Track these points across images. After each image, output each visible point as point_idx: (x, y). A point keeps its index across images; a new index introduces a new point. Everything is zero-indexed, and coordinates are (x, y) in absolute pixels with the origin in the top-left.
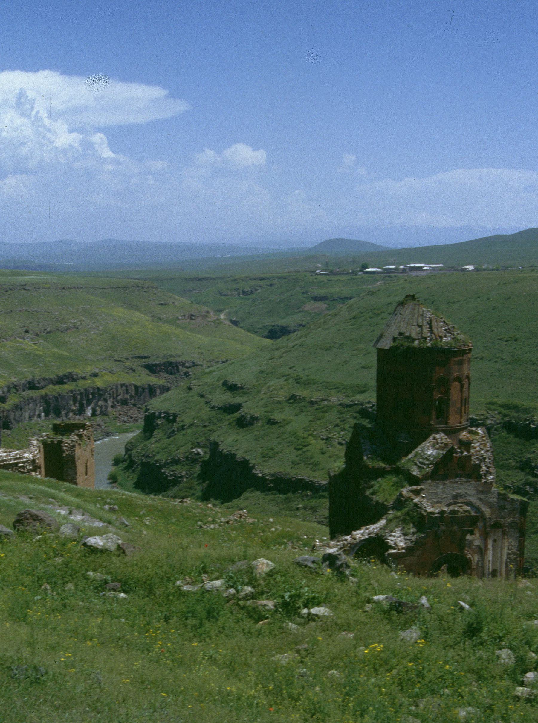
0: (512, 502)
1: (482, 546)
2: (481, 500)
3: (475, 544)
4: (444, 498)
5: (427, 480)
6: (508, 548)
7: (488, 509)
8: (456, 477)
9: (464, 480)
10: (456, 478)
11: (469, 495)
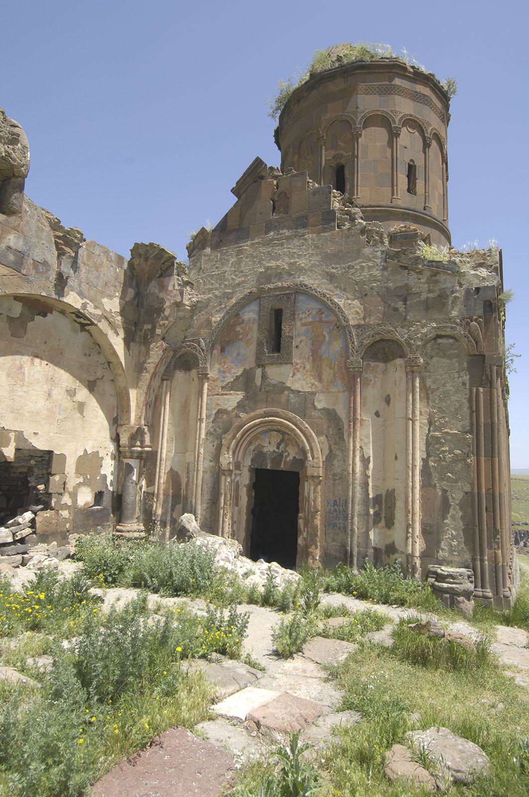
0: (435, 274)
1: (342, 413)
2: (332, 278)
3: (319, 406)
4: (238, 285)
5: (204, 248)
6: (430, 423)
7: (356, 302)
8: (268, 229)
9: (286, 232)
10: (266, 233)
11: (301, 270)
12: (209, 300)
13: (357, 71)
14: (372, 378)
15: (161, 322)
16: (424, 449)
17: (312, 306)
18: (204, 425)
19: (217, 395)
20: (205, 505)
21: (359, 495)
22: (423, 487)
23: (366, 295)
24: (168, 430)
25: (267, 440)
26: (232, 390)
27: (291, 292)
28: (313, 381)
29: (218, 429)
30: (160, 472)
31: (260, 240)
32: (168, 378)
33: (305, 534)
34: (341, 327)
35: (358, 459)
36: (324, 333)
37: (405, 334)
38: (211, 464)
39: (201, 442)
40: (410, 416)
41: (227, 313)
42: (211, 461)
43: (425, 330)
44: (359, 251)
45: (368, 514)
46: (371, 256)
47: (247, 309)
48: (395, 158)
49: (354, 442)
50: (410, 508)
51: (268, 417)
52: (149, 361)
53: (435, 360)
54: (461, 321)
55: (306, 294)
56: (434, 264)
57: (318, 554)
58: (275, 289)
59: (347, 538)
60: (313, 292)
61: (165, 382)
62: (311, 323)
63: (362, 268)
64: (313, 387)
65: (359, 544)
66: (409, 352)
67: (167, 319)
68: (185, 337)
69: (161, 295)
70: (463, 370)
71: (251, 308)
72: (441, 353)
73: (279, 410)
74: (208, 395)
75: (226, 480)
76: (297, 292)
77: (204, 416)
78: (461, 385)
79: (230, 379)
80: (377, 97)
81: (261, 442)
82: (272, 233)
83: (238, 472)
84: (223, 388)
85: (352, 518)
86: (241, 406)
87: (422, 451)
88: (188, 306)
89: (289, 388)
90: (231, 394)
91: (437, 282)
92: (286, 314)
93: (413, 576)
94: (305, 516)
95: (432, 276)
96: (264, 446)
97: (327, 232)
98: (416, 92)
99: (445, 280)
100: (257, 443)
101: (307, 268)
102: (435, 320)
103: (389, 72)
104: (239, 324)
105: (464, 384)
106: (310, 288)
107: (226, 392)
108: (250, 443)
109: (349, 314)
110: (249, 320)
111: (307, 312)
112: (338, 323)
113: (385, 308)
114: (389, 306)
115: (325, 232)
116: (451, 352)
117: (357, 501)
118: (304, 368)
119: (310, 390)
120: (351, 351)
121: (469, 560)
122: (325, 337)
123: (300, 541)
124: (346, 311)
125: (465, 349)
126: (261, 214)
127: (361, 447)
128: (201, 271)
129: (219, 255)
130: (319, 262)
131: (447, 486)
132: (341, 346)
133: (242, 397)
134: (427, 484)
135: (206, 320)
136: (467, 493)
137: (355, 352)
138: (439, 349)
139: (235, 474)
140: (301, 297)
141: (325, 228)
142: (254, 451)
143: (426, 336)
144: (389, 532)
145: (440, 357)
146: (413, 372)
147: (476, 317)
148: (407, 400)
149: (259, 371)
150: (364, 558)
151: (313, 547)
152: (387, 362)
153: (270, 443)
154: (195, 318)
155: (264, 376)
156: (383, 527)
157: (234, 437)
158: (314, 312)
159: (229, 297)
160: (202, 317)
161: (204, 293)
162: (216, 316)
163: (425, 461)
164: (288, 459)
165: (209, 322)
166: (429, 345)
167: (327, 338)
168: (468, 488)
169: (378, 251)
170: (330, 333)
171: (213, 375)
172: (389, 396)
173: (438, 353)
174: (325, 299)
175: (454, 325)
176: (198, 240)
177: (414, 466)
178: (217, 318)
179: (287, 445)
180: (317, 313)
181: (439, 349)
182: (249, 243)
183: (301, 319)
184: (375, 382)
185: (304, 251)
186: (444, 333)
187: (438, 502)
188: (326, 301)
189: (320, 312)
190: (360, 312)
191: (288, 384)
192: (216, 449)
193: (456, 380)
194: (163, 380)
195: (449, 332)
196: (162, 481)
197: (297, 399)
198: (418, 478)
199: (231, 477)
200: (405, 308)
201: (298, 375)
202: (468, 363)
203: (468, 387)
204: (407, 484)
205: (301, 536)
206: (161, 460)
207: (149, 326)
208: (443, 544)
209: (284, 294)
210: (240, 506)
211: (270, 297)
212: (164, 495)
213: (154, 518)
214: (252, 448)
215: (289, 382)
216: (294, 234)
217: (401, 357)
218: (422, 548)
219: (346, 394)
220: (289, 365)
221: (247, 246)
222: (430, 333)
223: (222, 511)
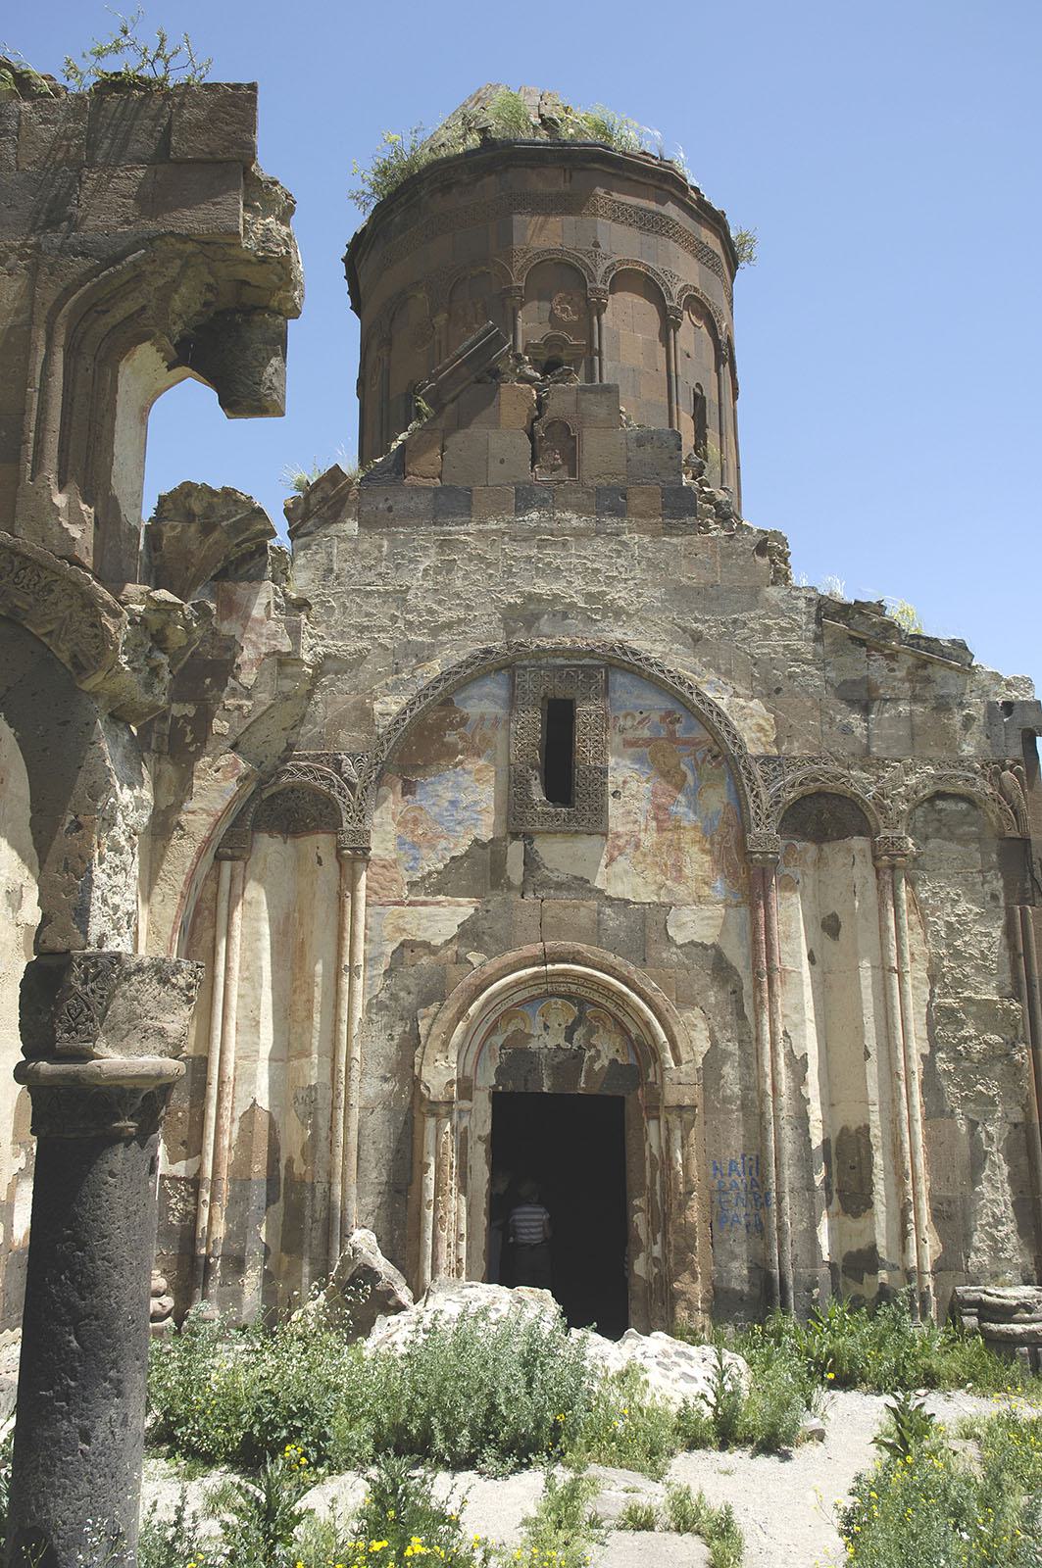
0: (924, 664)
1: (736, 955)
3: (680, 939)
4: (449, 626)
5: (336, 517)
6: (934, 977)
7: (756, 704)
9: (575, 520)
10: (520, 510)
12: (361, 657)
13: (596, 166)
14: (799, 877)
15: (230, 702)
16: (925, 1035)
17: (648, 702)
18: (359, 984)
19: (396, 904)
20: (371, 1201)
21: (789, 1147)
22: (927, 1117)
23: (778, 691)
24: (240, 996)
25: (539, 1019)
26: (439, 892)
27: (596, 662)
28: (660, 878)
29: (402, 994)
30: (219, 1116)
31: (503, 525)
32: (237, 854)
33: (657, 1250)
34: (721, 754)
35: (782, 1062)
36: (683, 767)
37: (870, 783)
38: (387, 1087)
39: (356, 1030)
40: (894, 964)
41: (422, 695)
42: (385, 1079)
43: (912, 780)
44: (755, 591)
45: (810, 1186)
46: (783, 606)
47: (473, 691)
48: (673, 374)
49: (772, 1021)
50: (908, 1165)
51: (554, 962)
52: (190, 805)
53: (933, 843)
54: (983, 767)
55: (633, 672)
56: (922, 642)
57: (698, 1290)
58: (555, 652)
59: (768, 1247)
60: (655, 670)
61: (227, 866)
62: (648, 742)
63: (767, 630)
64: (662, 892)
65: (795, 1260)
66: (882, 824)
67: (249, 697)
68: (290, 747)
69: (226, 628)
70: (991, 868)
71: (486, 690)
72: (944, 830)
73: (582, 947)
74: (367, 905)
75: (438, 1129)
76: (611, 665)
77: (360, 960)
78: (988, 899)
79: (433, 862)
80: (633, 232)
81: (521, 1026)
82: (535, 515)
83: (466, 1104)
84: (412, 885)
85: (780, 1201)
86: (469, 934)
87: (920, 1038)
88: (309, 667)
89: (601, 891)
90: (438, 903)
91: (928, 680)
92: (586, 711)
93: (924, 1316)
94: (651, 1201)
95: (917, 667)
96: (532, 1035)
97: (677, 535)
98: (701, 243)
99: (944, 678)
100: (511, 1028)
101: (632, 609)
102: (931, 761)
103: (656, 187)
104: (453, 726)
105: (994, 897)
106: (647, 659)
107: (422, 898)
108: (493, 1030)
109: (743, 729)
110: (482, 718)
111: (637, 714)
112: (716, 748)
113: (822, 723)
114: (832, 720)
115: (671, 535)
116: (966, 829)
117: (786, 1159)
118: (637, 846)
119: (655, 899)
120: (752, 813)
121: (1031, 1267)
122: (685, 776)
123: (640, 1267)
124: (735, 723)
125: (991, 824)
126: (502, 461)
127: (785, 1033)
128: (333, 576)
129: (385, 543)
130: (662, 601)
131: (976, 1113)
132: (725, 801)
133: (472, 911)
134: (936, 1110)
135: (354, 708)
136: (1016, 1125)
137: (763, 817)
138: (939, 821)
139: (461, 1111)
140: (619, 679)
141: (672, 527)
142: (502, 1047)
143: (915, 793)
144: (860, 1224)
145: (945, 839)
146: (893, 868)
147: (1011, 762)
148: (883, 929)
149: (515, 850)
150: (809, 1290)
151: (686, 1277)
152: (822, 842)
153: (546, 1027)
154: (318, 697)
155: (531, 862)
156: (837, 1214)
157: (461, 1014)
158: (655, 717)
159: (423, 655)
160: (340, 698)
161: (342, 635)
162: (386, 699)
163: (928, 1061)
164: (597, 1067)
165: (365, 715)
166: (919, 812)
167: (690, 778)
168: (1017, 1116)
169: (798, 598)
170: (696, 768)
171: (379, 852)
172: (834, 917)
173: (938, 830)
174: (684, 690)
175: (970, 775)
176: (319, 495)
177: (909, 1072)
178: (389, 705)
179: (591, 1032)
180: (663, 719)
181: (938, 820)
182: (472, 527)
183: (622, 730)
184: (804, 887)
185: (622, 569)
186: (950, 789)
187: (963, 1149)
188: (688, 695)
189: (669, 717)
190: (767, 727)
191: (599, 884)
192: (400, 1046)
193: (978, 887)
194: (219, 858)
195: (961, 787)
196: (225, 1142)
197: (622, 919)
198: (917, 1099)
199: (451, 1120)
200: (867, 729)
201: (622, 864)
202: (999, 855)
203: (1002, 903)
204: (899, 1114)
205: (642, 1255)
206: (221, 1083)
207: (190, 710)
208: (977, 1239)
209: (575, 666)
210: (469, 1194)
211: (540, 668)
212: (232, 1180)
213: (203, 1251)
214: (498, 1040)
215: (598, 877)
216: (592, 525)
217: (861, 834)
218: (935, 1252)
219: (744, 910)
220: (596, 839)
221: (468, 534)
222: (924, 787)
223: (430, 1213)
